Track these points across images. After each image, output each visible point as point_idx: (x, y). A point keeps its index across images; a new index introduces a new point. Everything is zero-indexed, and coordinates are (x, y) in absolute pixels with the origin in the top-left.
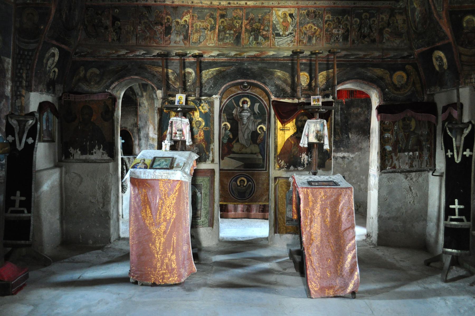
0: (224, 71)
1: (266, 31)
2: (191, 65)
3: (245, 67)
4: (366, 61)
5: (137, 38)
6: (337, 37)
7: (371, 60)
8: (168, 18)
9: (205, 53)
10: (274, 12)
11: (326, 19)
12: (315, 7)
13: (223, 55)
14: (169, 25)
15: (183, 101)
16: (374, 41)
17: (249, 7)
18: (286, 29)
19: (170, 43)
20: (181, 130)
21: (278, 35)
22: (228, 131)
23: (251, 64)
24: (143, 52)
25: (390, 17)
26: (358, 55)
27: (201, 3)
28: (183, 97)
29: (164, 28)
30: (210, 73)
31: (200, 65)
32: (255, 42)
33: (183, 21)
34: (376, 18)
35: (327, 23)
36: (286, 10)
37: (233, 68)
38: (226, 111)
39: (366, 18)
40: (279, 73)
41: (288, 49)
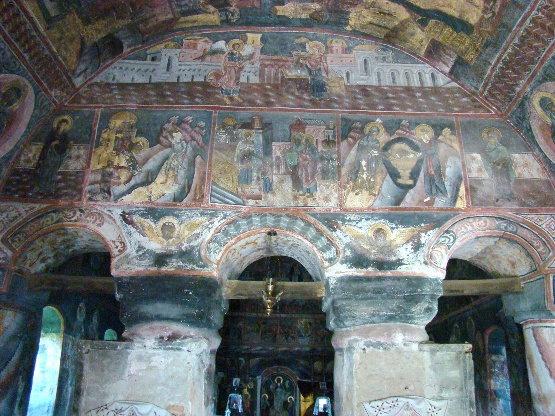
9: (252, 347)
15: (238, 383)
17: (282, 318)
20: (236, 402)
21: (301, 336)
22: (266, 401)
28: (238, 380)
31: (250, 356)
38: (266, 385)
40: (302, 362)
41: (307, 346)
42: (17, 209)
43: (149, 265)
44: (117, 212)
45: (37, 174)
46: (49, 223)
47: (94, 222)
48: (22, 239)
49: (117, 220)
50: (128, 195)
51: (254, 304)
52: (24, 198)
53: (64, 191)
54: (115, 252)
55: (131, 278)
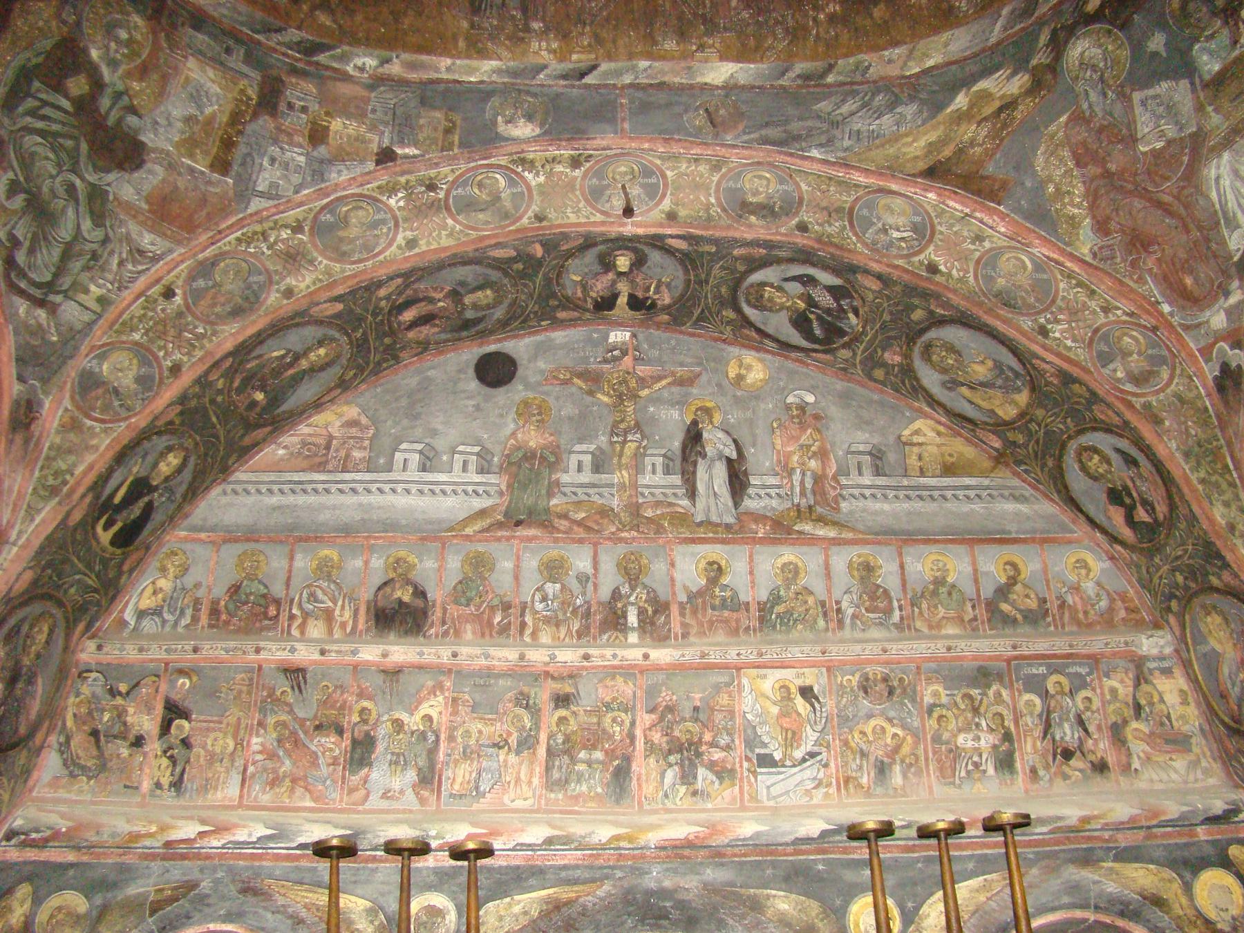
0: (569, 903)
1: (723, 749)
2: (440, 880)
3: (653, 885)
4: (1090, 838)
5: (243, 781)
6: (976, 759)
7: (1106, 835)
8: (364, 709)
9: (495, 833)
10: (745, 681)
11: (928, 700)
12: (887, 663)
13: (566, 840)
14: (367, 734)
16: (1101, 767)
17: (658, 668)
18: (792, 738)
19: (368, 795)
21: (766, 761)
23: (675, 871)
24: (264, 831)
25: (1137, 684)
26: (1060, 818)
27: (487, 656)
29: (346, 743)
30: (517, 909)
32: (683, 789)
33: (418, 716)
34: (1094, 690)
35: (935, 715)
37: (607, 887)
39: (1062, 693)
51: (506, 607)
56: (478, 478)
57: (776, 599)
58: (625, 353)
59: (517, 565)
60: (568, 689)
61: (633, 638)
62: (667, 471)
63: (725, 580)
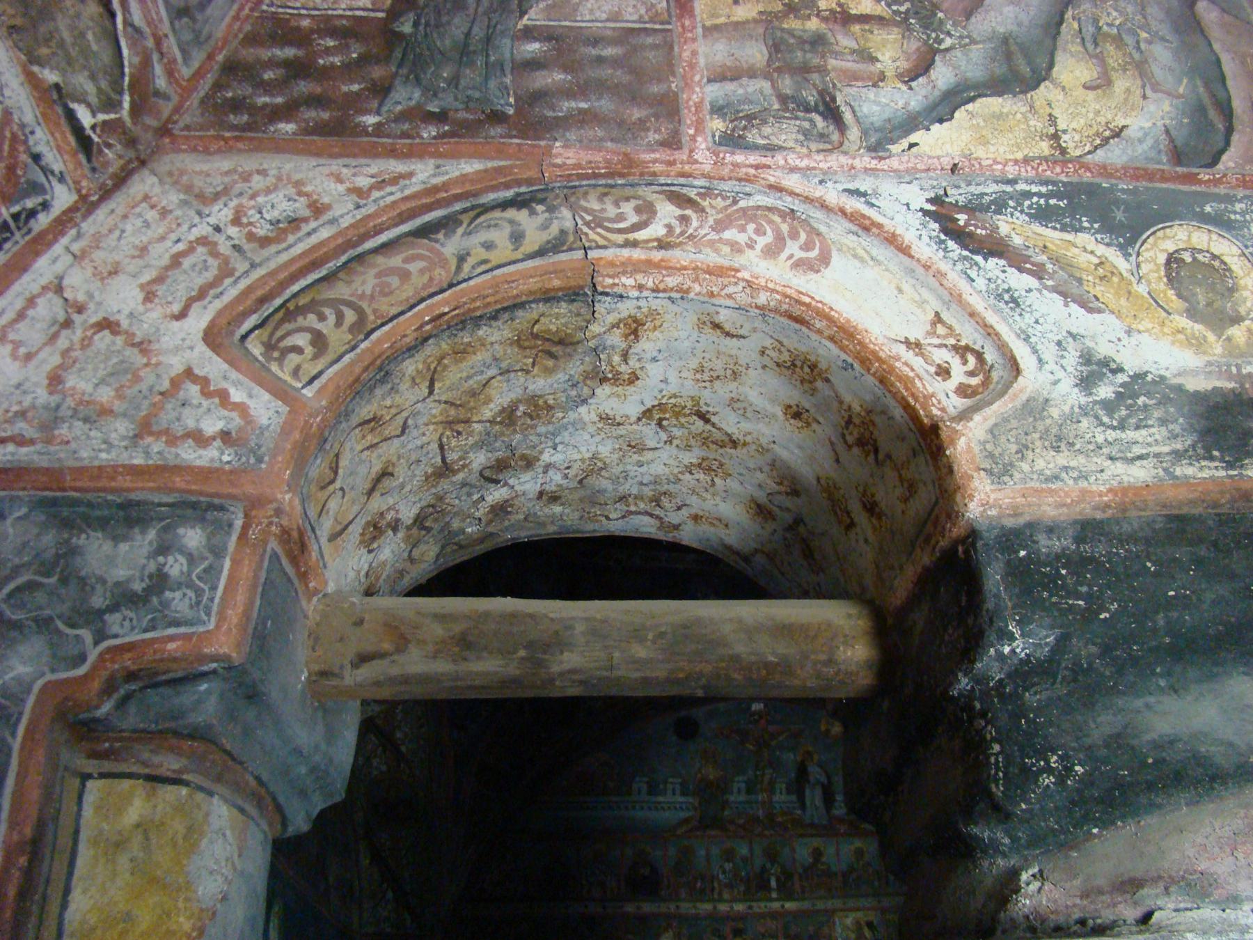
17: (789, 913)
27: (695, 907)
36: (860, 914)
42: (298, 184)
43: (1178, 455)
44: (901, 204)
45: (400, 36)
46: (495, 257)
47: (771, 252)
48: (337, 338)
49: (909, 237)
50: (936, 127)
52: (336, 132)
53: (567, 105)
54: (941, 397)
55: (1087, 529)
56: (681, 799)
57: (852, 869)
58: (761, 717)
59: (707, 852)
60: (741, 926)
61: (774, 895)
62: (789, 792)
63: (824, 859)
